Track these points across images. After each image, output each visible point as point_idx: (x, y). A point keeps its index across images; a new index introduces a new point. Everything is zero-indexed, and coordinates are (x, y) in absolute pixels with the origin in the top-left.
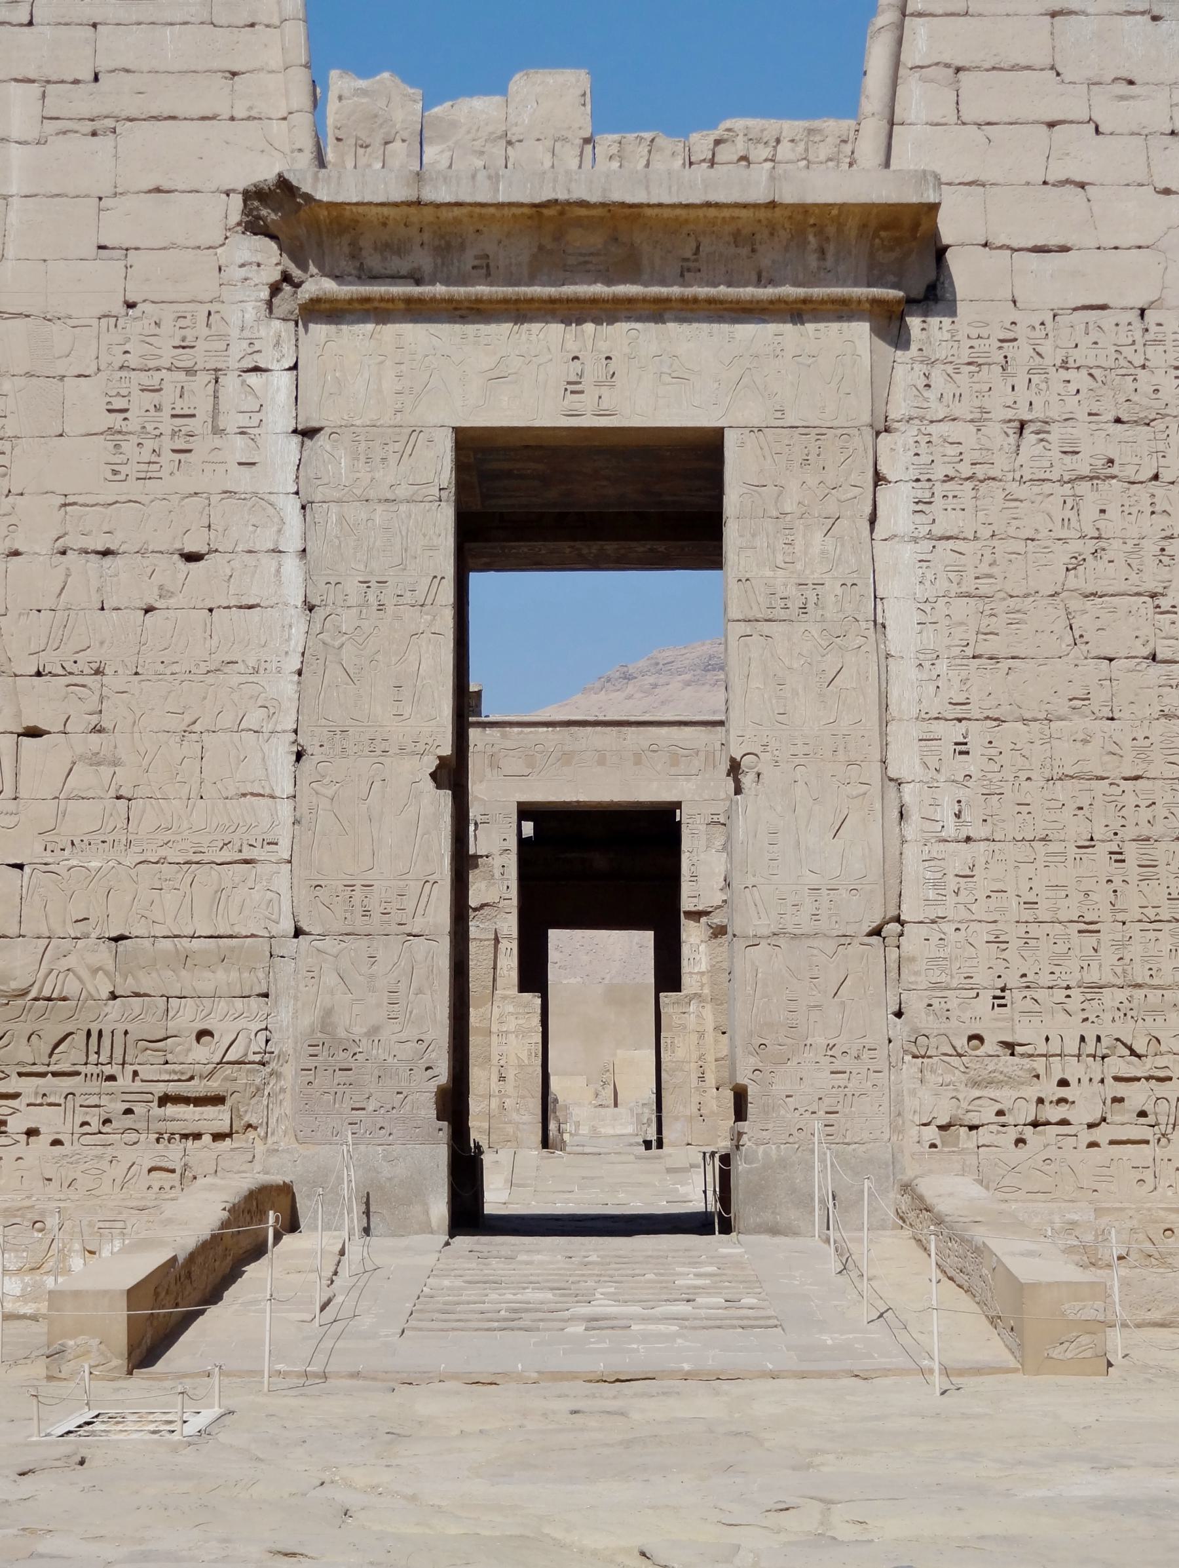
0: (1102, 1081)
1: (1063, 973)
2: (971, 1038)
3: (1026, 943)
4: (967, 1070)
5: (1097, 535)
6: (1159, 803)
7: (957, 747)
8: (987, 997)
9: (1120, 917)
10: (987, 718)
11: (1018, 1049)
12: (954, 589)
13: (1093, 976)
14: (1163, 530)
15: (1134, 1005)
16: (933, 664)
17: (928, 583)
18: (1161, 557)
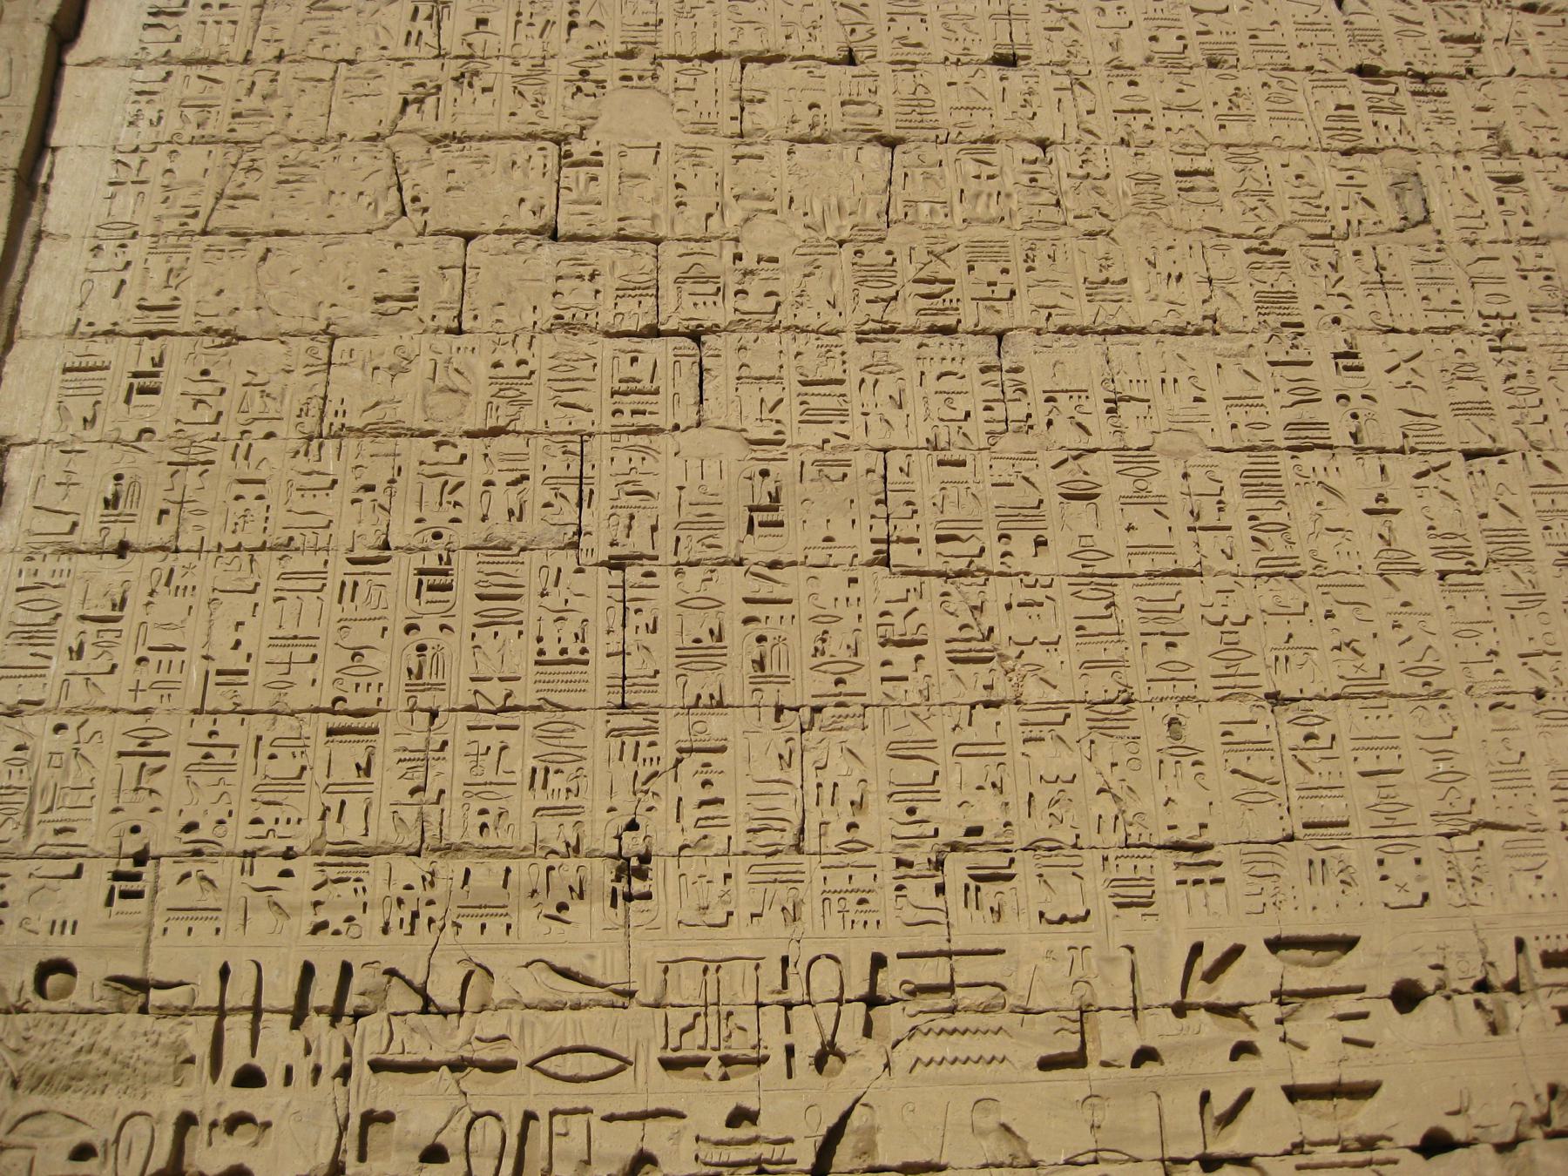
0: (345, 1073)
1: (283, 821)
2: (46, 969)
3: (207, 756)
4: (25, 1047)
5: (467, 52)
6: (537, 476)
7: (136, 381)
8: (98, 877)
9: (425, 700)
10: (208, 331)
11: (154, 993)
12: (191, 131)
13: (352, 828)
14: (588, 47)
15: (437, 892)
16: (123, 246)
17: (143, 124)
18: (580, 84)
